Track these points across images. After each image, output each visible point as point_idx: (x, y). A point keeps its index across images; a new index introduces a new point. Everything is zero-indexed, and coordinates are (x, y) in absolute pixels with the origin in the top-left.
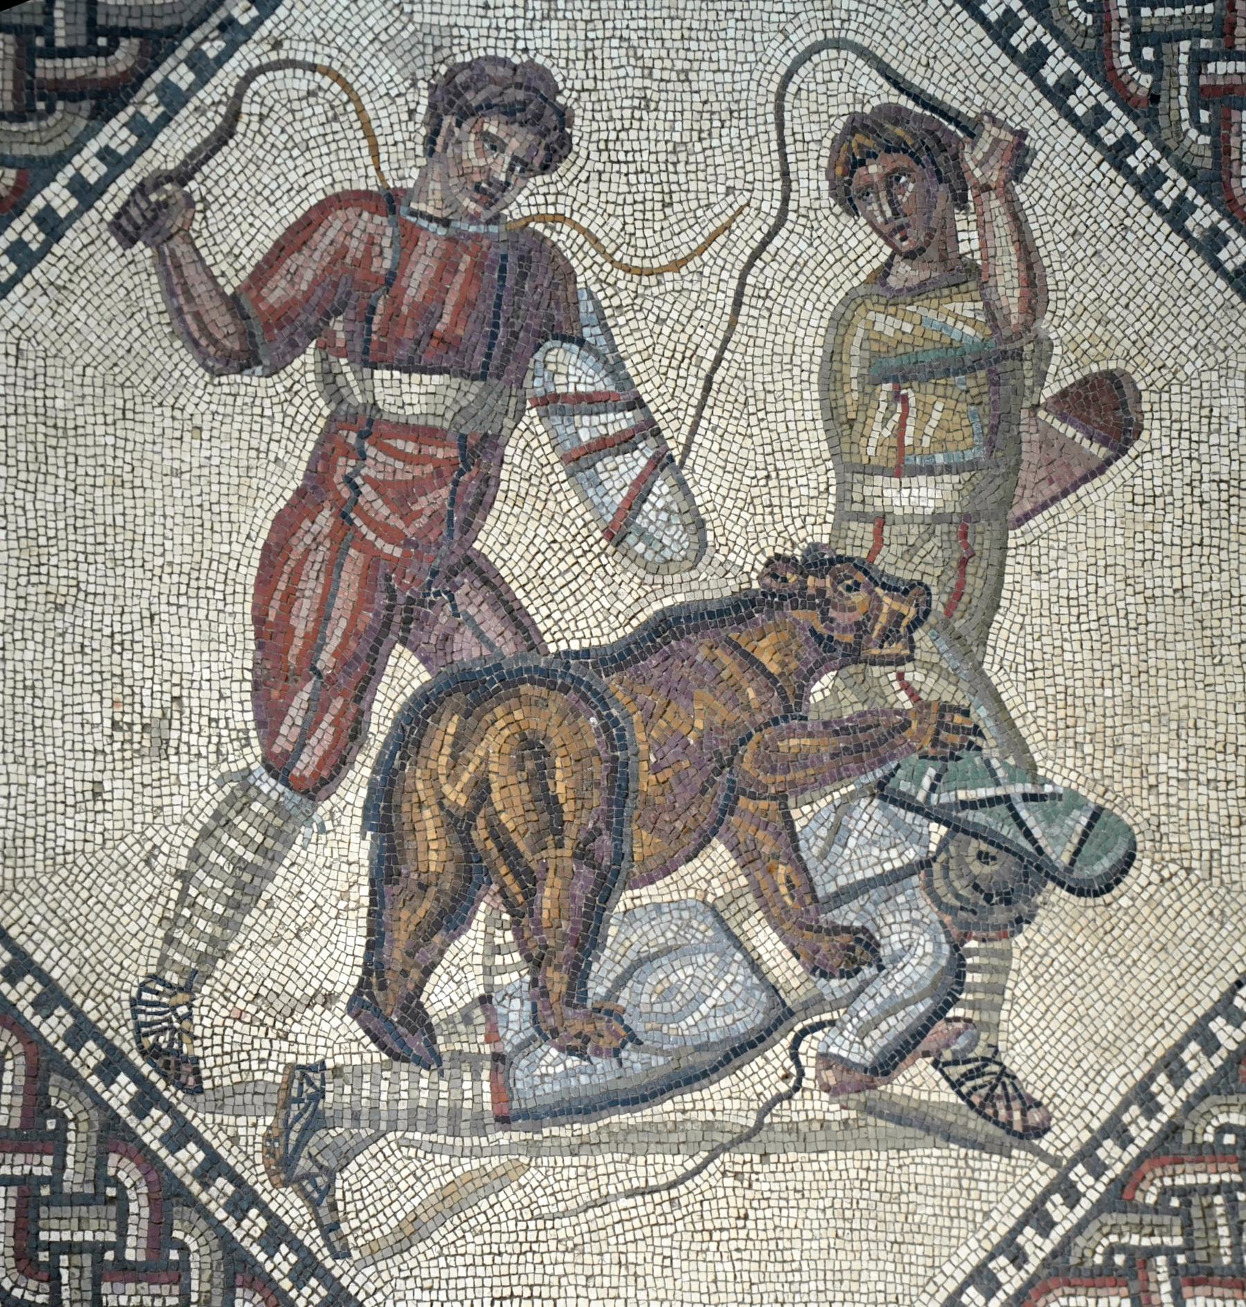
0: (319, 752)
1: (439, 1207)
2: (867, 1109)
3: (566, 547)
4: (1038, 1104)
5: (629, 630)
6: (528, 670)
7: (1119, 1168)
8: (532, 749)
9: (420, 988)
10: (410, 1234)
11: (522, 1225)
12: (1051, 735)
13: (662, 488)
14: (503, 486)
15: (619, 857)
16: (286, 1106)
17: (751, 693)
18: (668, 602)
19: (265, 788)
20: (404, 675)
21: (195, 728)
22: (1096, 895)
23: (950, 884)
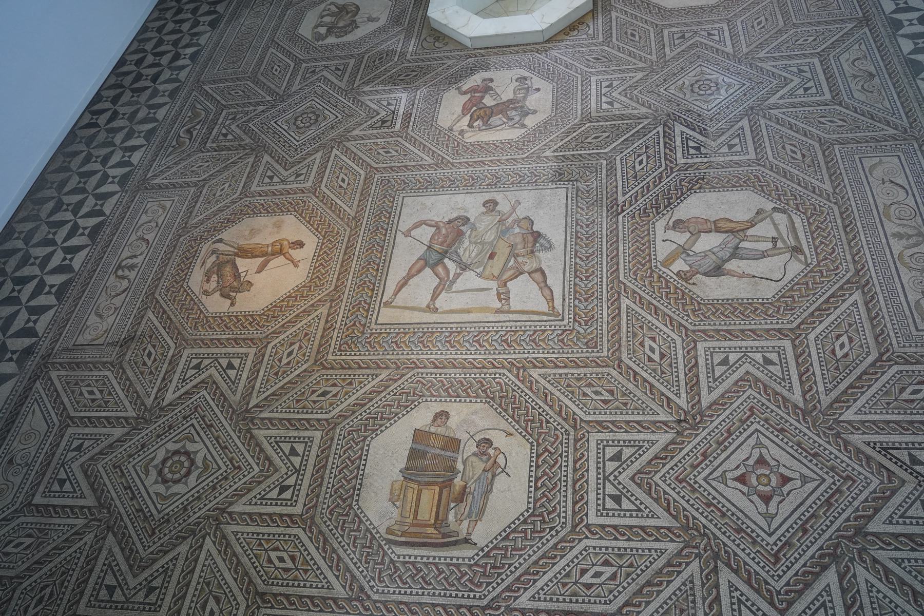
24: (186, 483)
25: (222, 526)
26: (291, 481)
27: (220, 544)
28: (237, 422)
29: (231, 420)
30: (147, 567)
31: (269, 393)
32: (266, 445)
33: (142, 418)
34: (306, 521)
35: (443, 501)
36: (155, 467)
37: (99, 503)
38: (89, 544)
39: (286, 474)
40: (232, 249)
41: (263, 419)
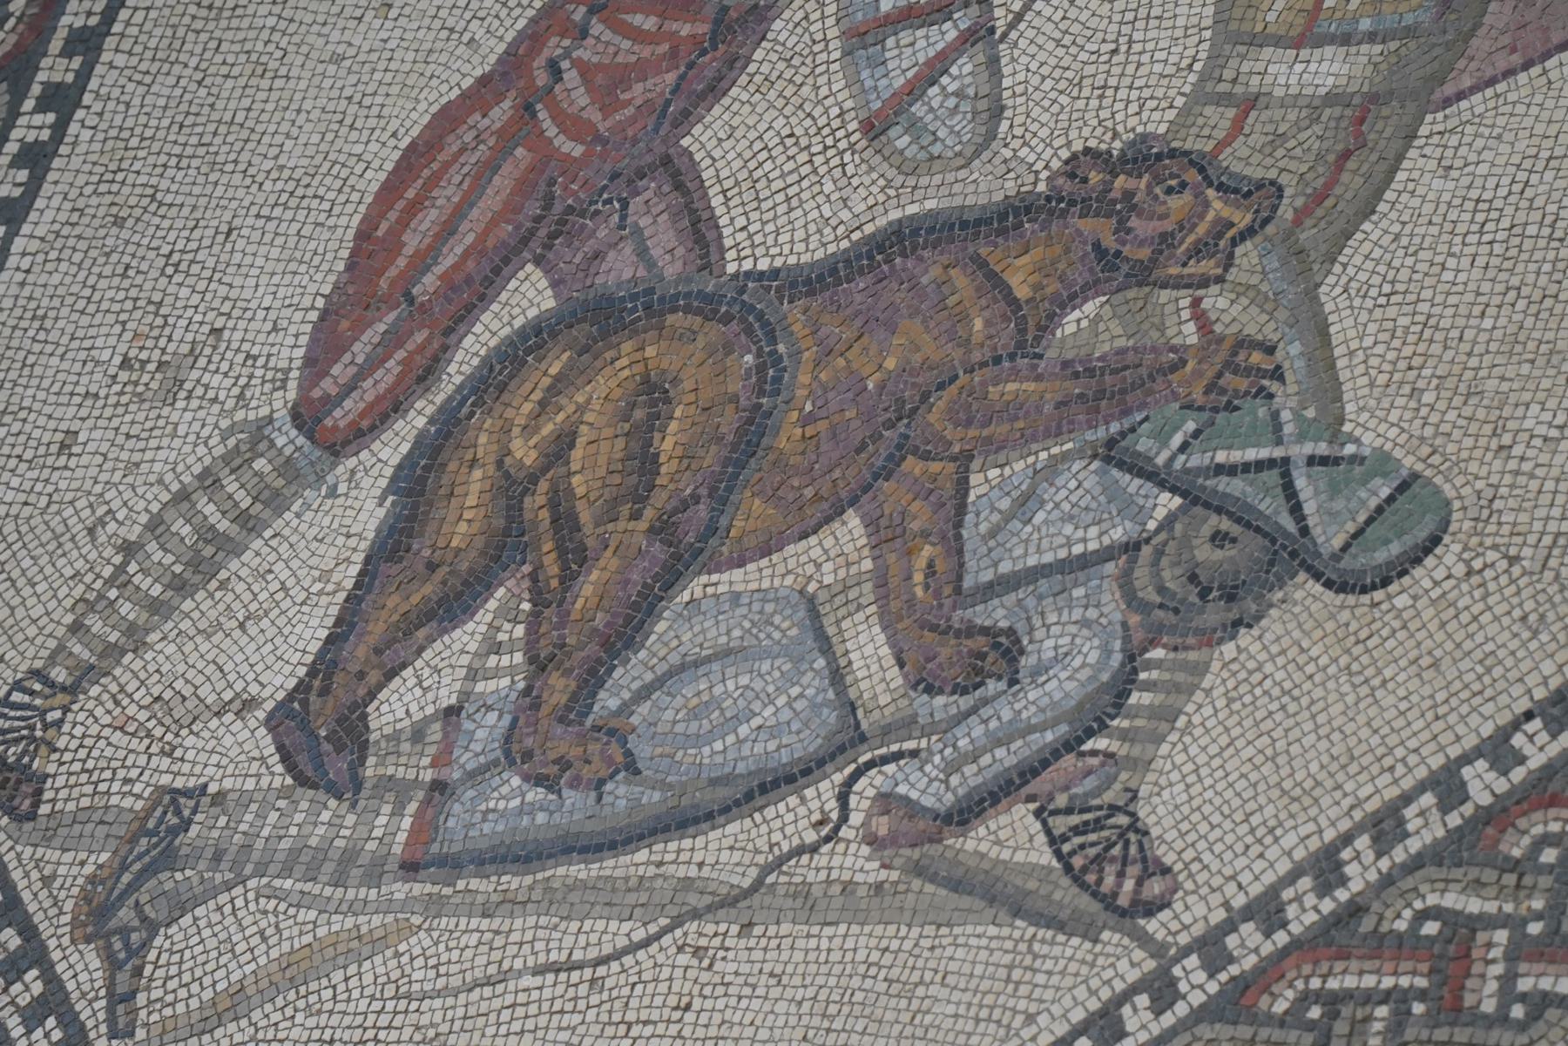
0: (369, 397)
1: (277, 978)
2: (918, 870)
3: (804, 142)
4: (1166, 871)
5: (845, 244)
6: (688, 295)
7: (1250, 962)
9: (372, 695)
11: (377, 1006)
12: (1382, 379)
13: (963, 67)
14: (752, 68)
15: (712, 530)
16: (133, 840)
17: (978, 324)
18: (912, 209)
19: (280, 442)
20: (529, 295)
21: (224, 366)
22: (1364, 590)
23: (1157, 574)
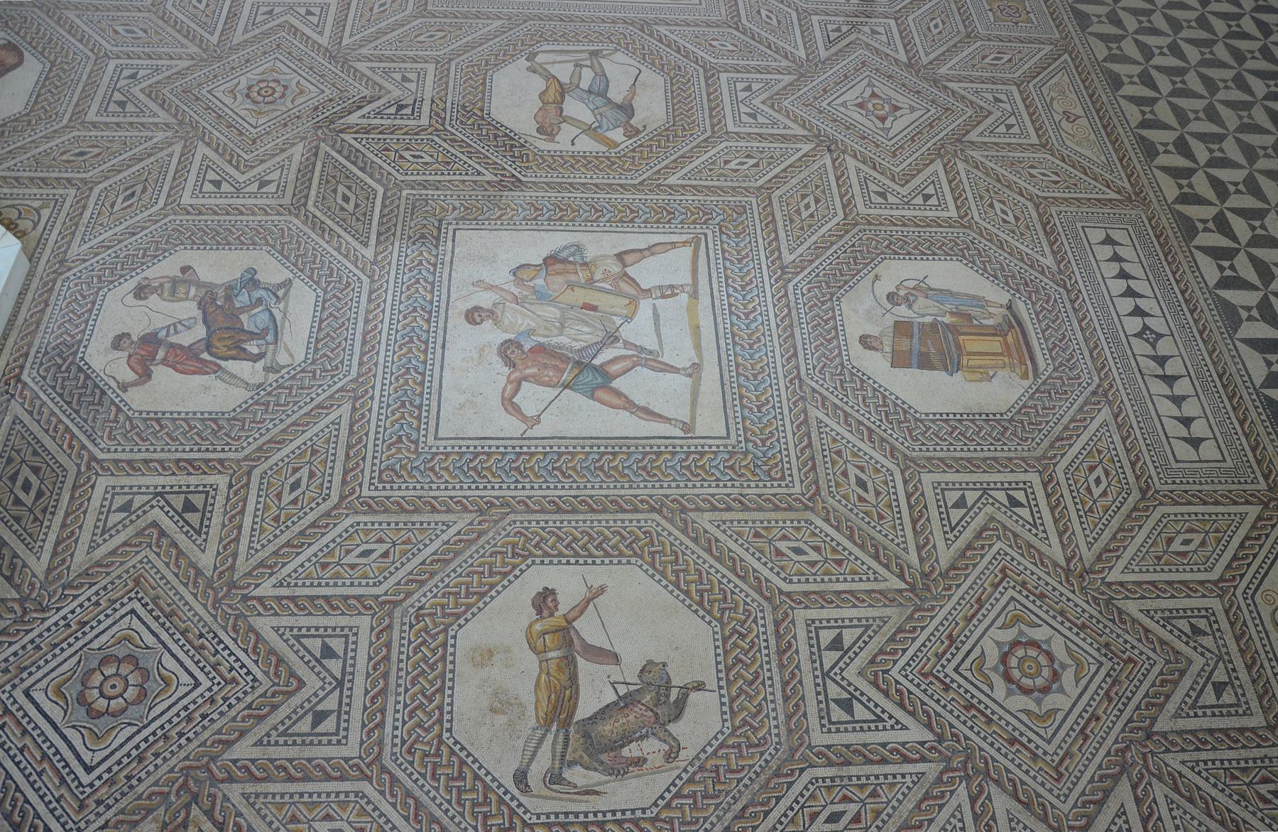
8: (219, 340)
10: (291, 355)
20: (205, 356)
24: (1048, 641)
25: (1087, 566)
26: (1001, 496)
27: (1108, 560)
28: (935, 598)
29: (933, 608)
30: (1173, 648)
31: (874, 565)
32: (961, 543)
33: (966, 769)
34: (1045, 466)
35: (973, 331)
36: (1038, 702)
37: (1121, 773)
38: (1182, 756)
39: (993, 504)
40: (550, 737)
41: (921, 560)
